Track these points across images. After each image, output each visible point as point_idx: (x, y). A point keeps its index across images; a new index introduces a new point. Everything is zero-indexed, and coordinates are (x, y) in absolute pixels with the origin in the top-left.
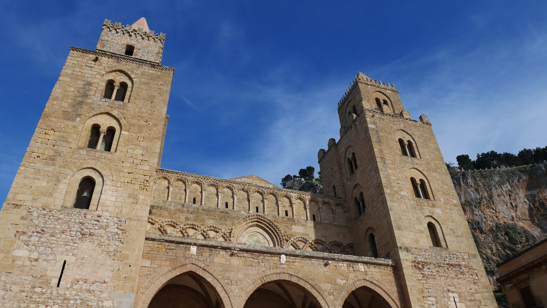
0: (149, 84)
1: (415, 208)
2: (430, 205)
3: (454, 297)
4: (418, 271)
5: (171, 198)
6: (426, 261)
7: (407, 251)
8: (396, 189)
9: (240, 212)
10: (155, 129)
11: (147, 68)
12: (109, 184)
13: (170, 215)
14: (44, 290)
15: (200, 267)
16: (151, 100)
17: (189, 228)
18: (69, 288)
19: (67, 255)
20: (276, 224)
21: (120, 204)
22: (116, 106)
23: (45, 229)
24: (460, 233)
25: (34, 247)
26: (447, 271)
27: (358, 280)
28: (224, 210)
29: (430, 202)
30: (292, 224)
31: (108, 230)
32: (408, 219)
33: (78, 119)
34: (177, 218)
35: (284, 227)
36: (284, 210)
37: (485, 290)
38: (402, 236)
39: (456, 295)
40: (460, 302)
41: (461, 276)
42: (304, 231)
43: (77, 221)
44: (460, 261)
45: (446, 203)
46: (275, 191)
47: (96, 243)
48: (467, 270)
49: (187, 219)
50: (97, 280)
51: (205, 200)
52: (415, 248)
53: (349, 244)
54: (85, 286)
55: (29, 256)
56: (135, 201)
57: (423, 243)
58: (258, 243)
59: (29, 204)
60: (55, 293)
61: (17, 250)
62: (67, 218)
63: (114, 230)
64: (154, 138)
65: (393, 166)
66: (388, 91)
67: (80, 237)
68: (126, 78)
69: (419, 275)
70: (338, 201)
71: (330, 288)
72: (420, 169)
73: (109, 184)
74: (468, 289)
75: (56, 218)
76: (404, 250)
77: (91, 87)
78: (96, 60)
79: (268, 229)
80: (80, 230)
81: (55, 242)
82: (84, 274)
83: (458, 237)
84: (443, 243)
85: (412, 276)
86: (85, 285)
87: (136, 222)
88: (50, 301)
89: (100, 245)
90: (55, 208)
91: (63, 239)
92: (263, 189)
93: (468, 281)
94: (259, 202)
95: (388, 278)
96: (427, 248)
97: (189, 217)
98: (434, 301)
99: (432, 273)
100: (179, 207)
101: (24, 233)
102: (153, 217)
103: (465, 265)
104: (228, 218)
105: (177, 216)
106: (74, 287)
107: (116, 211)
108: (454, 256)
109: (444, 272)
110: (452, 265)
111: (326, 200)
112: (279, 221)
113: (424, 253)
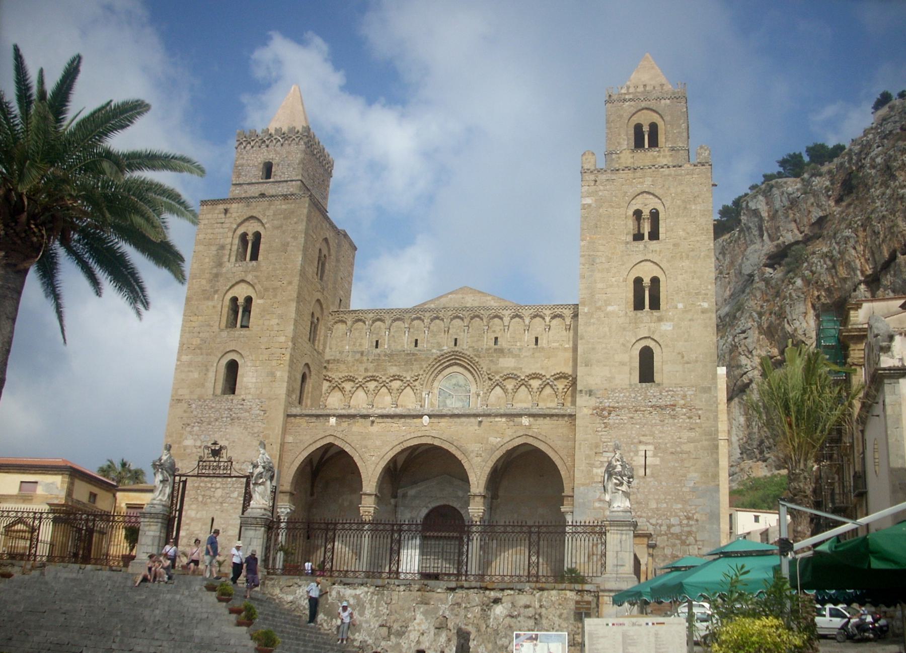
0: (281, 226)
1: (624, 329)
2: (654, 318)
4: (598, 420)
7: (590, 395)
8: (599, 304)
10: (290, 288)
11: (279, 203)
16: (285, 247)
17: (371, 380)
21: (260, 384)
22: (250, 268)
24: (694, 356)
31: (252, 412)
33: (216, 296)
35: (488, 362)
36: (493, 336)
37: (704, 438)
39: (651, 447)
40: (655, 456)
41: (671, 421)
45: (685, 311)
46: (482, 311)
49: (366, 370)
51: (389, 341)
59: (187, 397)
62: (218, 406)
64: (289, 300)
66: (663, 101)
68: (259, 224)
69: (598, 425)
73: (249, 364)
76: (586, 394)
78: (226, 211)
79: (469, 367)
83: (688, 363)
84: (657, 377)
85: (587, 427)
89: (246, 428)
93: (681, 426)
95: (560, 431)
101: (189, 425)
102: (329, 374)
104: (415, 360)
105: (356, 368)
107: (258, 392)
110: (660, 407)
111: (558, 311)
112: (481, 355)
113: (617, 395)
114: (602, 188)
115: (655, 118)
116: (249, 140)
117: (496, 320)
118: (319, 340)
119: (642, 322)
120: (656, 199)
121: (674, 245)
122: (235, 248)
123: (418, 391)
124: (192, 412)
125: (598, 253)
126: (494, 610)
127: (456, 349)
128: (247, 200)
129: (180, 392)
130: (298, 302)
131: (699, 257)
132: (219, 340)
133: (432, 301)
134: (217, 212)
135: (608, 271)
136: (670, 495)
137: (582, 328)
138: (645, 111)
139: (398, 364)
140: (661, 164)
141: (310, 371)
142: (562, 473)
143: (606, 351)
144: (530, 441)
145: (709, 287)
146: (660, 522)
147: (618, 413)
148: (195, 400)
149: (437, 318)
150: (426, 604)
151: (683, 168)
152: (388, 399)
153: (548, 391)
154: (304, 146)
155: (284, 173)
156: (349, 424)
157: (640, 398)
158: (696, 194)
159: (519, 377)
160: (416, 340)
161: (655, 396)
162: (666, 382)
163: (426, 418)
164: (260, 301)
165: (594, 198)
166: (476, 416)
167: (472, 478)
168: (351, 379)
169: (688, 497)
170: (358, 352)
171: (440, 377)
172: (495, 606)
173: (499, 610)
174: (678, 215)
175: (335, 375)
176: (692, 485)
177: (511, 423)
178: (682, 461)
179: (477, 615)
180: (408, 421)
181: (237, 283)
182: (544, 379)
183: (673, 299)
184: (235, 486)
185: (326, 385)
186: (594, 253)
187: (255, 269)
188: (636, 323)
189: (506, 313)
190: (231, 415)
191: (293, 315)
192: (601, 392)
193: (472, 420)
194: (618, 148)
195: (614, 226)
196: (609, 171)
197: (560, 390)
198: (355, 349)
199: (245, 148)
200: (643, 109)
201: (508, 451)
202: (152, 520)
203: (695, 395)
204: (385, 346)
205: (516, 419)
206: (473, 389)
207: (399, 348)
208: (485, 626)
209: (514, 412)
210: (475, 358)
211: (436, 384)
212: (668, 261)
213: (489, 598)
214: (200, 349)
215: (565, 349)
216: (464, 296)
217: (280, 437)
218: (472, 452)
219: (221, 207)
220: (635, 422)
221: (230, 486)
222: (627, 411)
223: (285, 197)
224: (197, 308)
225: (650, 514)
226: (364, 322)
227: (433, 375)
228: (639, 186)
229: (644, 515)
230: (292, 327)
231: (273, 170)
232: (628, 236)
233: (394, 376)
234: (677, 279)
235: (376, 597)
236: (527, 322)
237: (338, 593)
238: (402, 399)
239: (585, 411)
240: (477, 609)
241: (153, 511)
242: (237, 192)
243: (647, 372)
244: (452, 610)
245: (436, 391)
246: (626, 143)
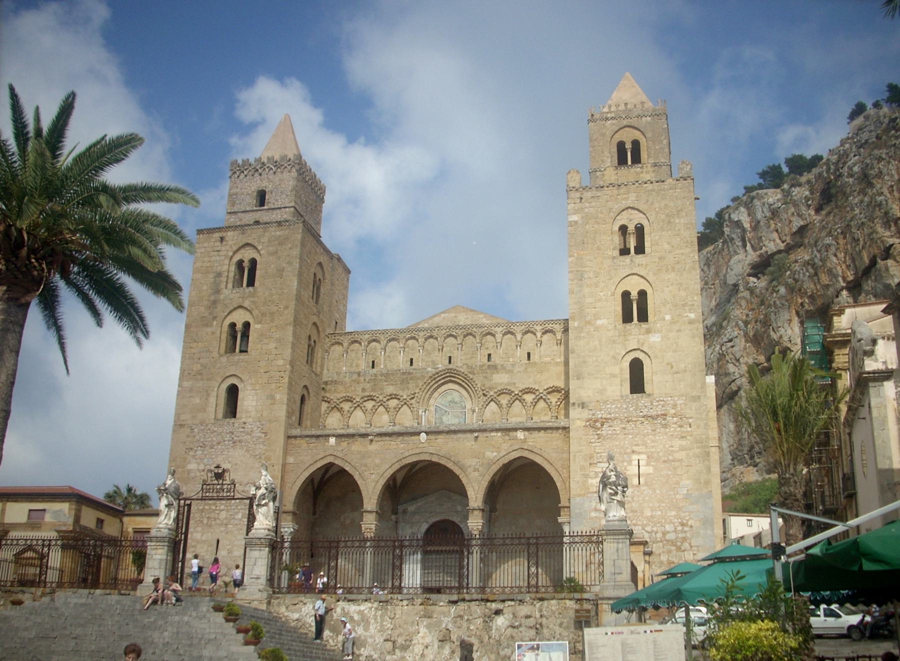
0: (276, 252)
1: (614, 342)
2: (643, 330)
4: (591, 431)
6: (609, 416)
7: (583, 408)
8: (588, 319)
9: (426, 369)
10: (286, 312)
11: (273, 229)
12: (249, 388)
16: (280, 272)
17: (368, 400)
20: (471, 376)
24: (682, 366)
30: (493, 373)
33: (215, 323)
37: (695, 446)
38: (580, 388)
40: (648, 464)
41: (662, 430)
45: (673, 322)
46: (474, 329)
49: (364, 390)
51: (385, 361)
59: (190, 422)
61: (189, 465)
62: (220, 430)
64: (286, 324)
66: (644, 119)
68: (255, 251)
69: (592, 437)
74: (667, 446)
77: (221, 279)
78: (222, 239)
79: (463, 384)
83: (677, 373)
84: (647, 388)
85: (581, 439)
89: (247, 451)
93: (672, 435)
96: (616, 398)
97: (366, 388)
100: (355, 377)
101: (192, 449)
102: (328, 395)
104: (411, 379)
105: (353, 388)
110: (651, 417)
111: (549, 327)
112: (475, 372)
114: (587, 205)
115: (637, 135)
116: (242, 169)
117: (489, 337)
118: (317, 362)
119: (630, 334)
120: (641, 215)
121: (660, 258)
122: (232, 275)
123: (415, 409)
124: (195, 437)
125: (586, 269)
126: (496, 621)
127: (451, 366)
128: (242, 228)
129: (183, 417)
130: (295, 326)
131: (684, 270)
132: (218, 365)
133: (425, 321)
134: (213, 240)
135: (597, 286)
136: (664, 503)
138: (627, 129)
139: (394, 383)
140: (644, 180)
141: (309, 393)
142: (558, 485)
145: (695, 298)
146: (655, 529)
147: (611, 424)
148: (197, 425)
149: (431, 337)
150: (429, 617)
151: (665, 183)
152: (386, 418)
153: (542, 404)
154: (296, 174)
155: (277, 200)
156: (348, 444)
157: (631, 409)
158: (679, 208)
159: (513, 392)
160: (412, 360)
161: (646, 407)
162: (656, 392)
163: (423, 435)
164: (258, 326)
165: (580, 215)
166: (472, 431)
167: (471, 493)
168: (349, 400)
169: (681, 504)
170: (355, 373)
171: (436, 394)
172: (496, 617)
173: (500, 621)
174: (662, 229)
175: (333, 396)
176: (685, 492)
177: (507, 438)
178: (675, 468)
179: (479, 626)
180: (406, 438)
181: (235, 309)
182: (537, 393)
183: (660, 311)
184: (239, 507)
185: (324, 406)
186: (582, 269)
187: (252, 295)
188: (625, 336)
189: (499, 330)
190: (233, 438)
191: (291, 339)
193: (469, 435)
194: (602, 166)
195: (600, 241)
196: (594, 188)
197: (554, 403)
198: (352, 370)
199: (238, 177)
200: (625, 127)
201: (504, 465)
202: (158, 544)
203: (685, 404)
204: (381, 366)
205: (511, 434)
206: (469, 405)
207: (395, 367)
208: (487, 637)
209: (509, 426)
210: (470, 375)
211: (432, 401)
212: (654, 274)
213: (490, 610)
214: (201, 374)
215: (557, 364)
217: (281, 458)
218: (470, 466)
219: (217, 235)
220: (627, 432)
221: (233, 507)
222: (619, 422)
223: (279, 223)
224: (197, 334)
225: (645, 522)
226: (360, 344)
227: (429, 393)
228: (623, 202)
229: (639, 523)
230: (290, 350)
231: (267, 197)
232: (615, 252)
233: (391, 395)
234: (663, 292)
235: (380, 612)
236: (519, 338)
237: (343, 609)
238: (400, 418)
239: (579, 423)
240: (479, 621)
241: (159, 534)
242: (232, 220)
243: (637, 384)
244: (455, 622)
245: (432, 409)
246: (609, 160)
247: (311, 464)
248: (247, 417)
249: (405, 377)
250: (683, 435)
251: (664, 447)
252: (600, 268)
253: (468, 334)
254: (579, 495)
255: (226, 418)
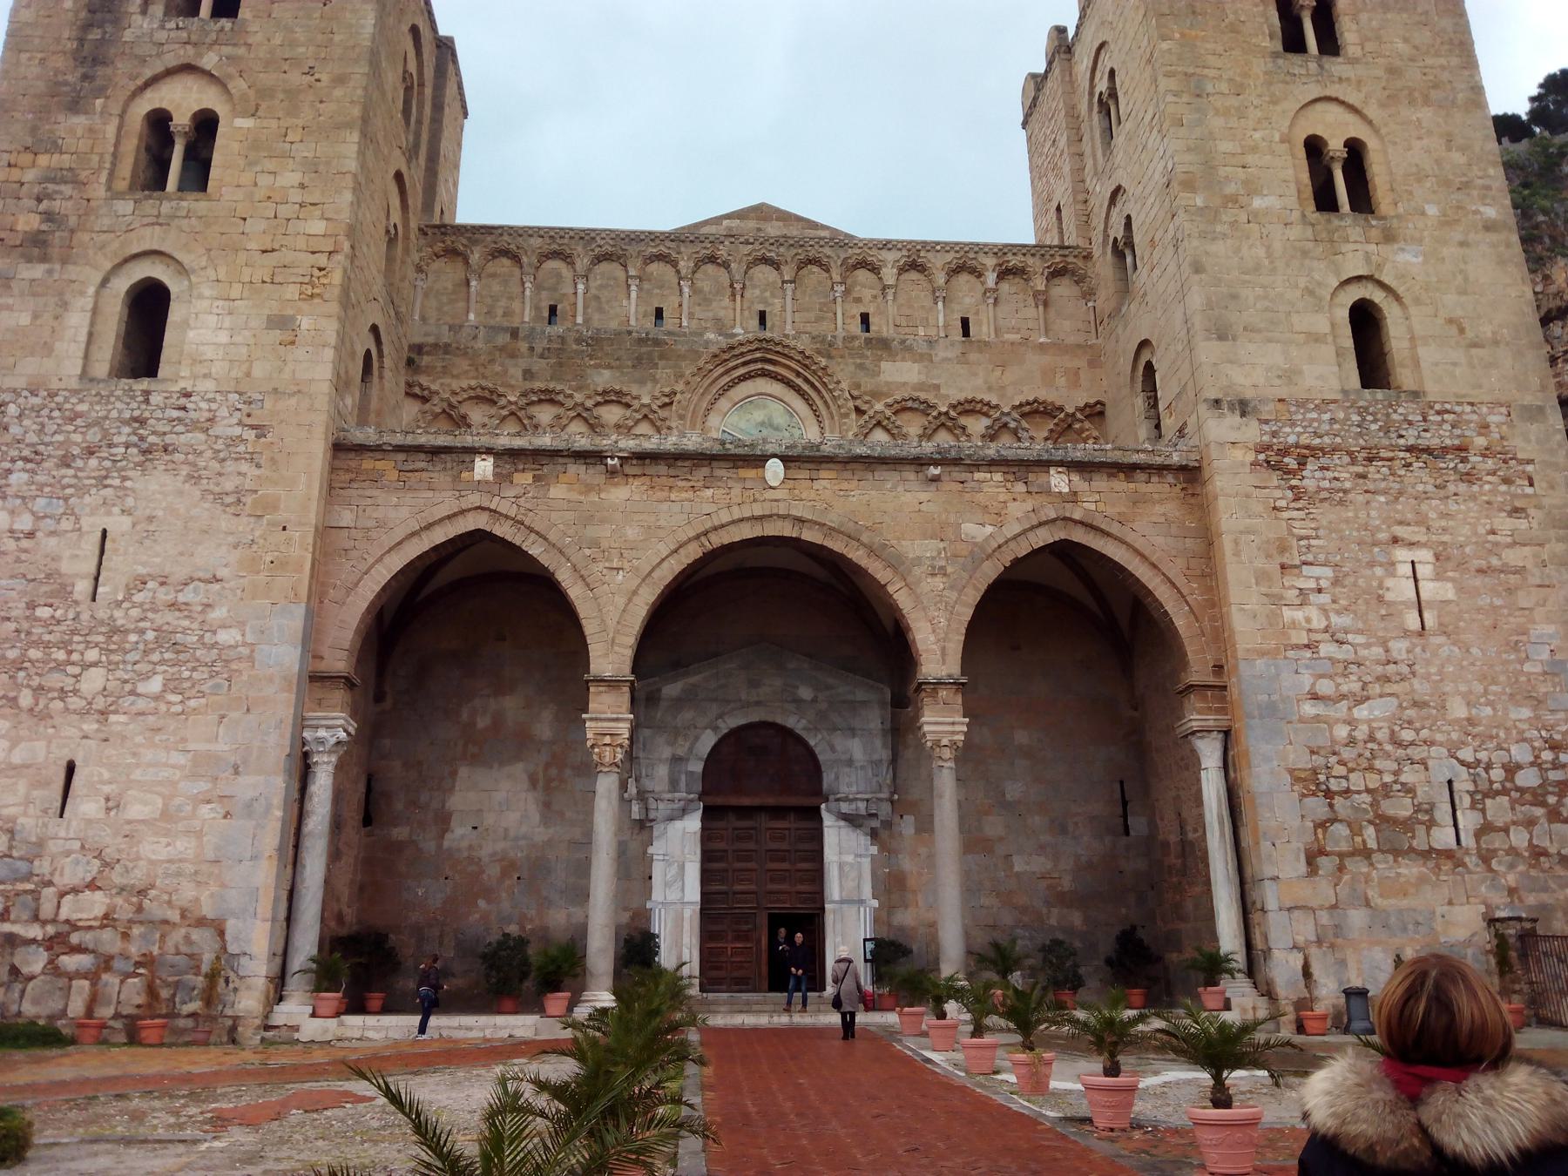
2: (1374, 233)
3: (1413, 562)
4: (1274, 478)
5: (477, 315)
6: (1317, 441)
7: (1243, 414)
8: (1231, 189)
9: (701, 335)
12: (207, 292)
13: (477, 369)
14: (59, 613)
15: (507, 517)
17: (540, 401)
18: (122, 602)
19: (109, 513)
21: (244, 350)
23: (41, 448)
25: (19, 501)
26: (1402, 472)
27: (1041, 524)
28: (647, 334)
29: (1374, 223)
30: (880, 359)
32: (1266, 297)
34: (497, 374)
35: (852, 368)
36: (857, 311)
38: (1231, 362)
39: (1424, 555)
40: (1438, 577)
41: (1462, 487)
42: (923, 378)
43: (127, 415)
44: (1467, 433)
45: (1446, 222)
46: (827, 251)
47: (184, 473)
48: (1490, 464)
49: (528, 374)
50: (196, 575)
51: (585, 307)
52: (1280, 400)
53: (1087, 405)
54: (164, 595)
55: (11, 525)
56: (288, 336)
57: (1317, 378)
58: (770, 429)
60: (85, 616)
63: (230, 429)
65: (1234, 101)
67: (137, 459)
69: (1278, 493)
70: (1058, 259)
71: (935, 554)
72: (1351, 102)
73: (207, 292)
74: (1482, 531)
75: (67, 413)
76: (1232, 408)
79: (799, 381)
80: (134, 439)
81: (73, 481)
82: (158, 560)
83: (1475, 345)
84: (1404, 376)
85: (1248, 496)
86: (163, 589)
87: (293, 401)
88: (76, 638)
89: (194, 478)
90: (62, 385)
91: (93, 470)
92: (782, 249)
93: (1488, 503)
94: (768, 294)
97: (535, 368)
98: (1326, 578)
99: (1337, 484)
102: (424, 380)
103: (1487, 449)
104: (662, 357)
105: (498, 368)
106: (135, 599)
107: (234, 374)
108: (1446, 416)
109: (1391, 478)
110: (1428, 450)
111: (1014, 261)
112: (834, 353)
113: (1314, 415)
121: (1393, 71)
125: (1211, 73)
127: (768, 335)
131: (1453, 102)
137: (1195, 243)
143: (1267, 303)
144: (1079, 536)
145: (1491, 171)
146: (1483, 755)
157: (1374, 427)
159: (934, 407)
161: (1410, 423)
163: (775, 468)
168: (488, 398)
169: (1543, 690)
170: (505, 330)
171: (724, 404)
176: (1545, 656)
177: (1020, 487)
181: (169, 73)
183: (1411, 193)
184: (155, 657)
186: (1198, 71)
191: (352, 165)
192: (1271, 406)
195: (1235, 13)
198: (492, 322)
201: (1017, 562)
203: (1511, 425)
207: (614, 325)
212: (1382, 105)
216: (762, 225)
217: (314, 506)
218: (918, 561)
220: (1371, 487)
221: (132, 657)
222: (1346, 459)
225: (1454, 736)
229: (1439, 737)
230: (348, 196)
233: (605, 392)
247: (413, 534)
248: (195, 377)
249: (644, 349)
250: (1518, 504)
251: (1475, 533)
252: (1246, 75)
253: (810, 261)
254: (1262, 654)
255: (119, 377)
